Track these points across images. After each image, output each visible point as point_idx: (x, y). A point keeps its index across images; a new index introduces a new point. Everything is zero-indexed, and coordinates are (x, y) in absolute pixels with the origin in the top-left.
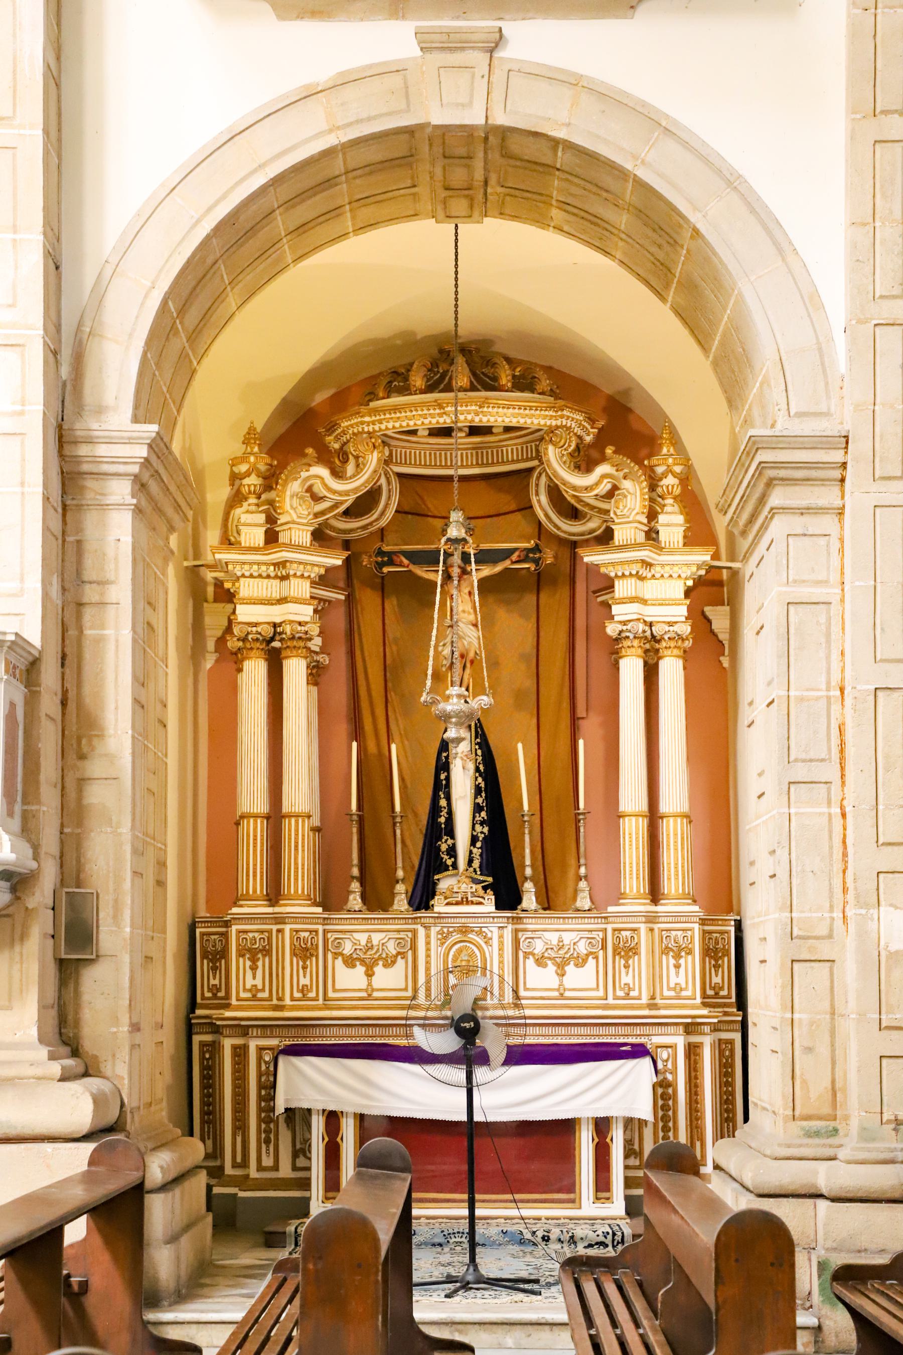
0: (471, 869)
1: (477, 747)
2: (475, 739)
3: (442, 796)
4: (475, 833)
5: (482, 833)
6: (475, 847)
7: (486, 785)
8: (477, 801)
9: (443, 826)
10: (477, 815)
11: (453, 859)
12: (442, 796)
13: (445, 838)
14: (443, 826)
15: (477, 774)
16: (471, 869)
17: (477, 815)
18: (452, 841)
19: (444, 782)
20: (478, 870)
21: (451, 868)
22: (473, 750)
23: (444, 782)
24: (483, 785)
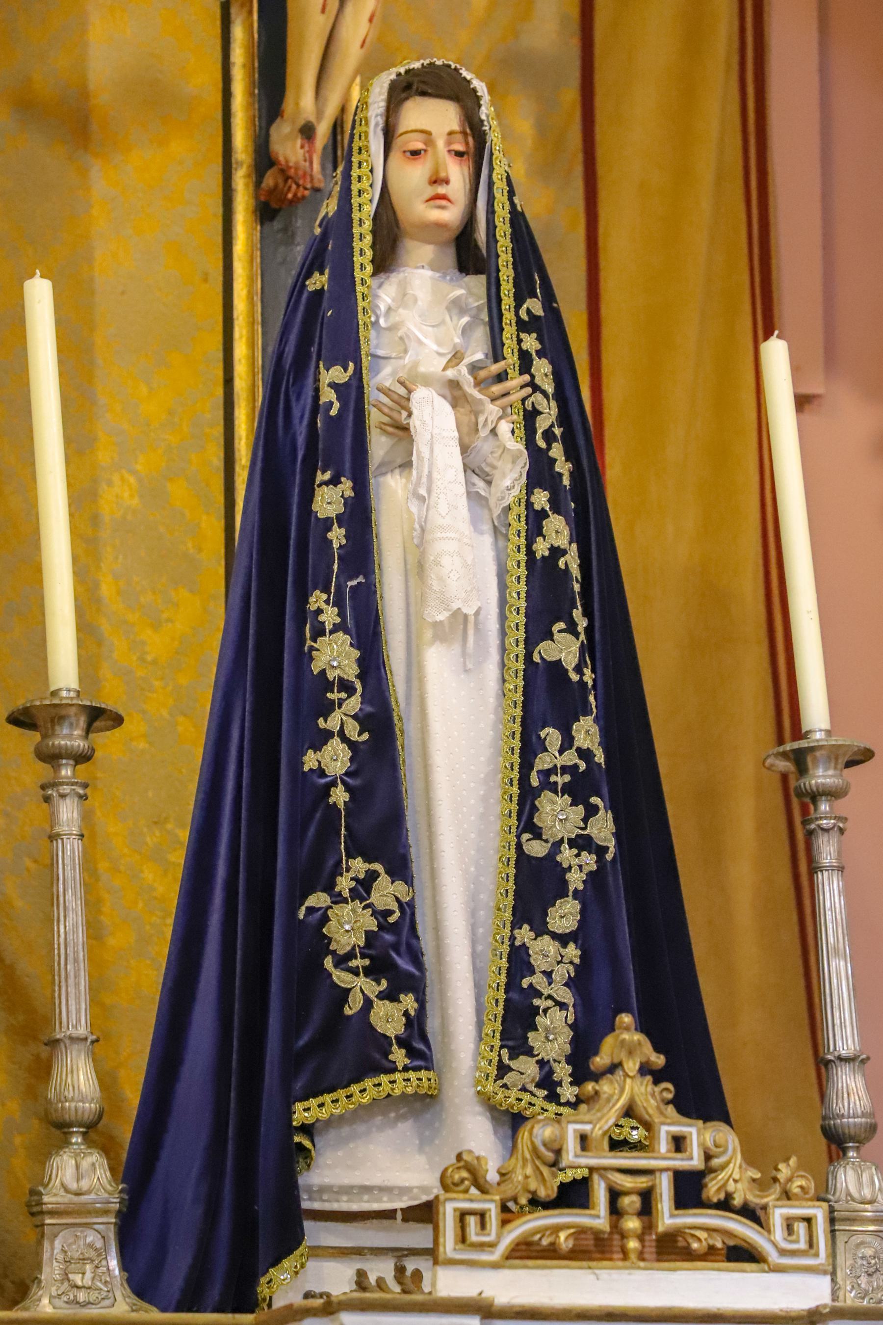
0: (527, 1067)
1: (531, 343)
2: (519, 301)
3: (330, 616)
4: (537, 849)
5: (582, 843)
6: (541, 930)
7: (585, 566)
8: (547, 651)
9: (339, 796)
10: (552, 736)
11: (409, 1002)
12: (330, 616)
13: (359, 866)
14: (339, 796)
15: (541, 499)
16: (527, 1067)
17: (552, 736)
18: (400, 888)
19: (337, 536)
20: (563, 1071)
21: (399, 1056)
22: (512, 359)
23: (337, 536)
24: (571, 561)
